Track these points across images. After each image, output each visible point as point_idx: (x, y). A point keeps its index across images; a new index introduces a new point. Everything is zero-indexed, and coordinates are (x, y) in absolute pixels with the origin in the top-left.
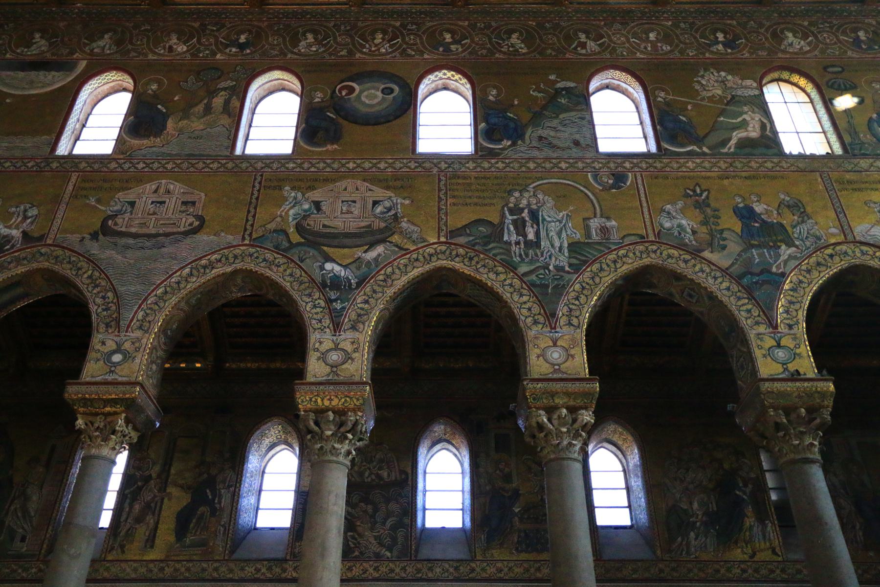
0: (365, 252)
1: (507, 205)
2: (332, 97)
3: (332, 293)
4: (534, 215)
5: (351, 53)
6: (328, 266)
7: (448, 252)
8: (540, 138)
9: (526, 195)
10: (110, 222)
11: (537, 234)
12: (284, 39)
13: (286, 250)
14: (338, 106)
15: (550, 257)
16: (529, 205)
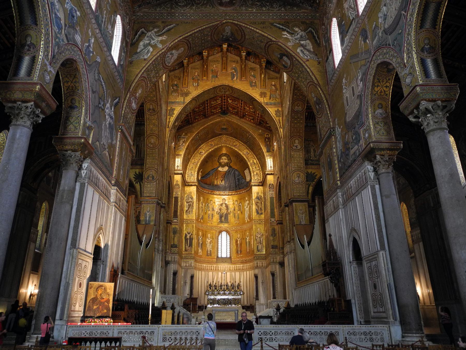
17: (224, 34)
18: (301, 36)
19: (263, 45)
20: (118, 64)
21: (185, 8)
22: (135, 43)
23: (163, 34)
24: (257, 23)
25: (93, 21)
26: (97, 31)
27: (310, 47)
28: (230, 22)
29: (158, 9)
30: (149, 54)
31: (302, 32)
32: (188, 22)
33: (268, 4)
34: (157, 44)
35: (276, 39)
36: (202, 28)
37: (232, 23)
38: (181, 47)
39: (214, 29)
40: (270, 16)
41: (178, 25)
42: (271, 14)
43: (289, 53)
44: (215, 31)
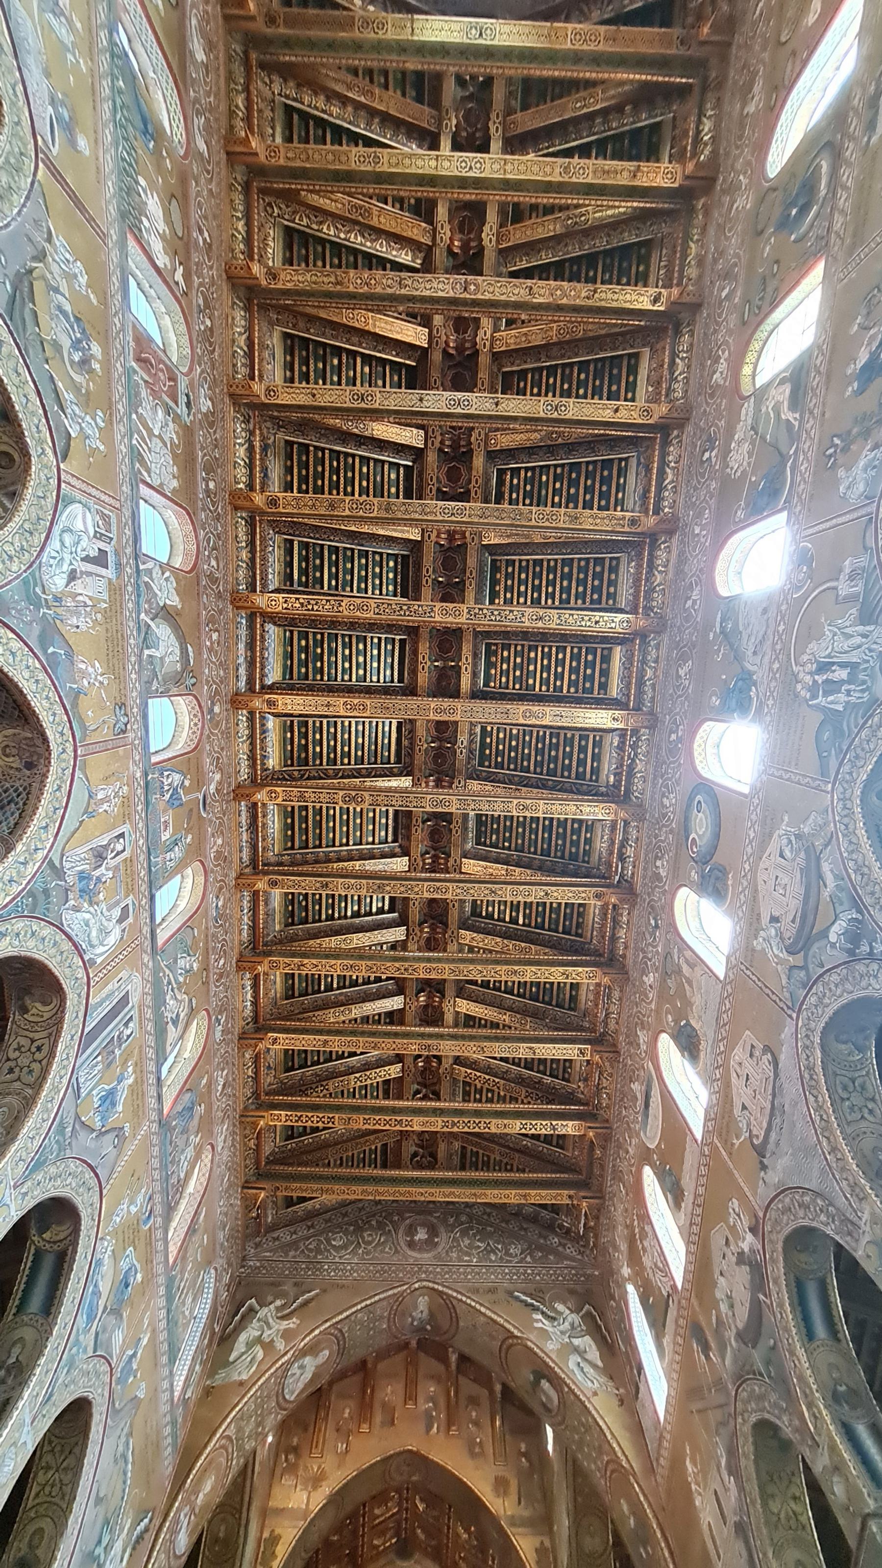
0: (826, 886)
1: (807, 701)
2: (696, 862)
3: (863, 948)
4: (824, 667)
5: (671, 831)
6: (833, 938)
7: (845, 785)
8: (755, 653)
9: (801, 675)
10: (755, 1142)
11: (843, 665)
12: (656, 886)
13: (808, 975)
14: (704, 859)
15: (871, 650)
16: (811, 673)
18: (572, 1325)
19: (496, 1344)
21: (343, 1252)
22: (230, 1335)
23: (292, 1313)
24: (481, 1291)
27: (594, 1354)
28: (428, 1288)
29: (292, 1253)
30: (254, 1368)
36: (373, 1300)
37: (433, 1289)
38: (323, 1349)
41: (324, 1291)
43: (552, 1369)
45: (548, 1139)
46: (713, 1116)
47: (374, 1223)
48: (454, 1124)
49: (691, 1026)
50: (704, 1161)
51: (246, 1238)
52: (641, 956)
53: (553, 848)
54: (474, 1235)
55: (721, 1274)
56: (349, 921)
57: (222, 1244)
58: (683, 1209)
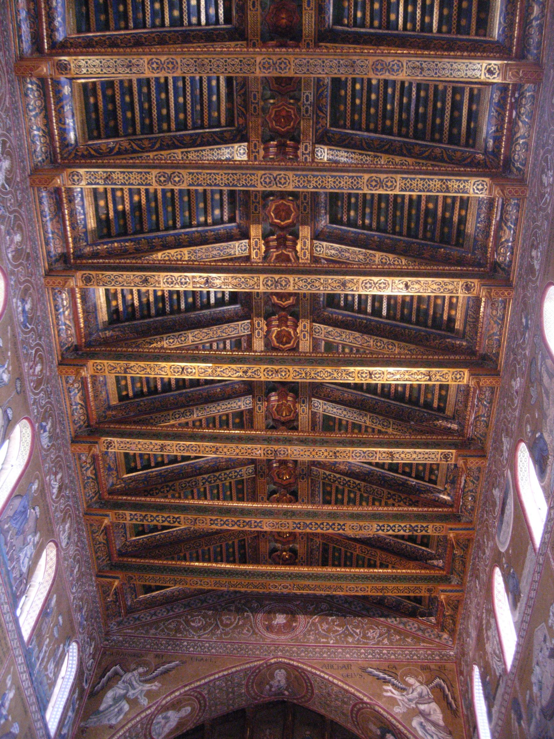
17: (272, 682)
18: (421, 695)
20: (56, 734)
24: (335, 667)
25: (20, 660)
26: (25, 676)
27: (438, 716)
28: (285, 663)
30: (121, 717)
31: (422, 687)
32: (205, 659)
33: (358, 631)
34: (139, 697)
35: (371, 699)
36: (230, 671)
38: (184, 707)
39: (253, 673)
40: (361, 654)
41: (184, 662)
42: (363, 651)
44: (254, 678)
45: (412, 539)
46: (549, 529)
47: (233, 608)
48: (306, 526)
49: (544, 439)
50: (538, 569)
51: (108, 617)
52: (512, 357)
53: (421, 228)
54: (333, 621)
55: (537, 664)
56: (182, 315)
57: (80, 624)
58: (518, 609)
